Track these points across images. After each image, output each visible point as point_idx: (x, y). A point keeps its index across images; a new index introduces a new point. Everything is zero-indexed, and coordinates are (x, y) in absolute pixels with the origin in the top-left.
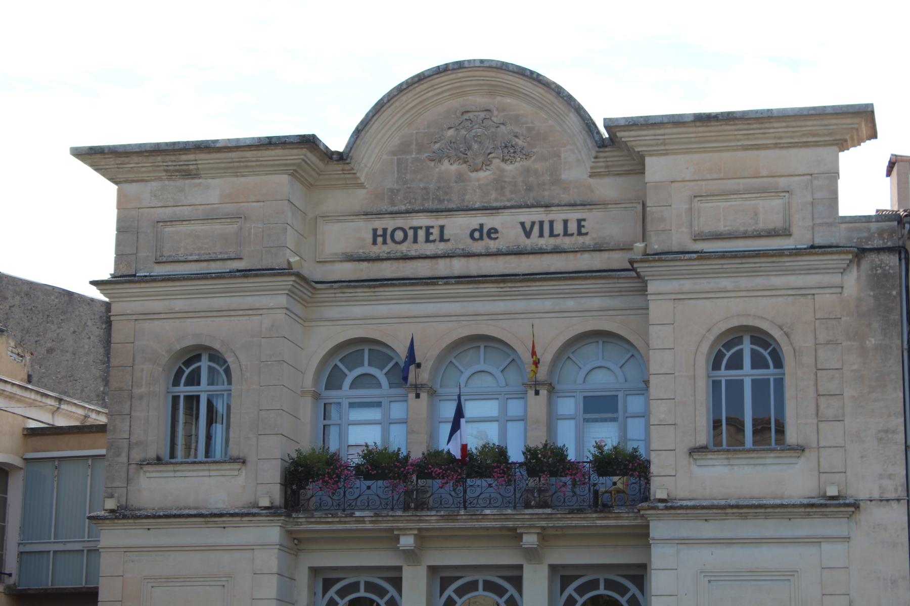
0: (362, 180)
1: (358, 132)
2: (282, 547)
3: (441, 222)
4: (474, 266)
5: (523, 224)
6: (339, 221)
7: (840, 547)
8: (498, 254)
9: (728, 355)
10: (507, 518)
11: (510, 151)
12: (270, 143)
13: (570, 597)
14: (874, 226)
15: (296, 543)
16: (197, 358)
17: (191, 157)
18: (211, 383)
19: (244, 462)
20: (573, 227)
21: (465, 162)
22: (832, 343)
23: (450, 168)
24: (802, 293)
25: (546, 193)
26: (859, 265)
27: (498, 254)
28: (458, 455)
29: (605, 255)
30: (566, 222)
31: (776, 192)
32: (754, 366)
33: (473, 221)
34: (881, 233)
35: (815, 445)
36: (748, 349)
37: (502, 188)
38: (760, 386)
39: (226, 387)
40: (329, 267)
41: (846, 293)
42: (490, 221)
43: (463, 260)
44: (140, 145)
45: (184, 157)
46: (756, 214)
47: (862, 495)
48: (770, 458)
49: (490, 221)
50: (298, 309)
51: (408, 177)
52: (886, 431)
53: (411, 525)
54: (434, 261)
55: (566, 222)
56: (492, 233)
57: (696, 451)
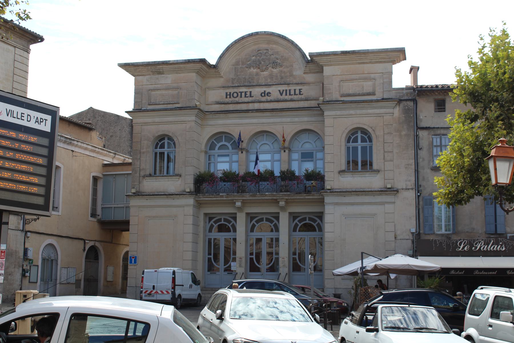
0: (222, 75)
1: (221, 57)
2: (194, 206)
3: (251, 90)
4: (262, 106)
5: (279, 91)
6: (214, 90)
7: (391, 206)
8: (271, 101)
9: (353, 138)
10: (274, 196)
11: (275, 64)
12: (189, 62)
13: (296, 223)
14: (405, 91)
15: (199, 205)
16: (164, 139)
17: (161, 67)
18: (168, 148)
19: (180, 176)
22: (390, 133)
23: (254, 70)
24: (379, 115)
25: (288, 80)
26: (399, 105)
27: (271, 101)
28: (256, 173)
29: (309, 102)
30: (295, 90)
31: (370, 79)
32: (362, 142)
34: (407, 94)
35: (383, 170)
36: (360, 136)
37: (272, 78)
38: (364, 149)
39: (174, 149)
40: (210, 106)
41: (395, 115)
42: (268, 90)
43: (258, 104)
44: (142, 62)
45: (158, 67)
46: (363, 87)
47: (399, 187)
48: (367, 174)
49: (268, 90)
50: (199, 121)
51: (239, 74)
52: (408, 165)
53: (240, 198)
54: (248, 104)
55: (295, 90)
56: (269, 93)
57: (341, 172)
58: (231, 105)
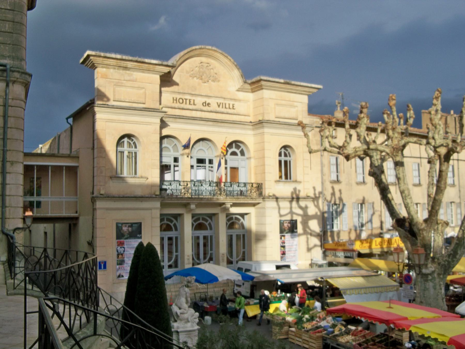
5: (217, 103)
20: (231, 107)
21: (202, 79)
30: (229, 104)
33: (204, 100)
42: (208, 101)
43: (200, 112)
55: (229, 104)
57: (276, 181)
58: (177, 110)
